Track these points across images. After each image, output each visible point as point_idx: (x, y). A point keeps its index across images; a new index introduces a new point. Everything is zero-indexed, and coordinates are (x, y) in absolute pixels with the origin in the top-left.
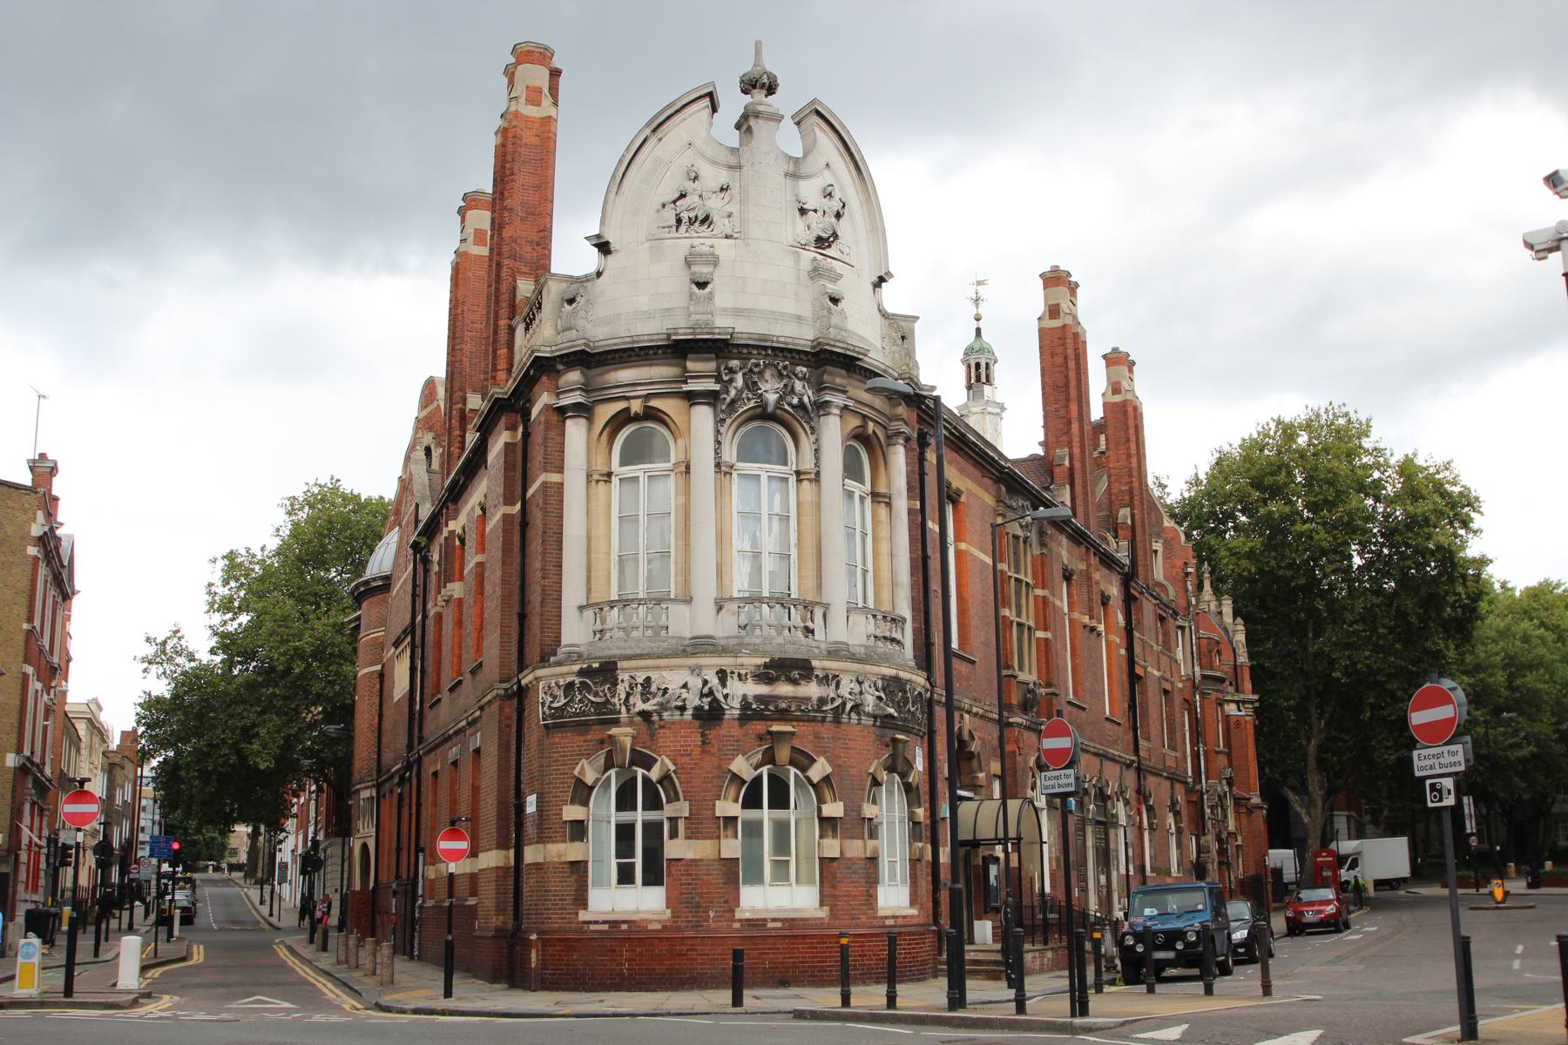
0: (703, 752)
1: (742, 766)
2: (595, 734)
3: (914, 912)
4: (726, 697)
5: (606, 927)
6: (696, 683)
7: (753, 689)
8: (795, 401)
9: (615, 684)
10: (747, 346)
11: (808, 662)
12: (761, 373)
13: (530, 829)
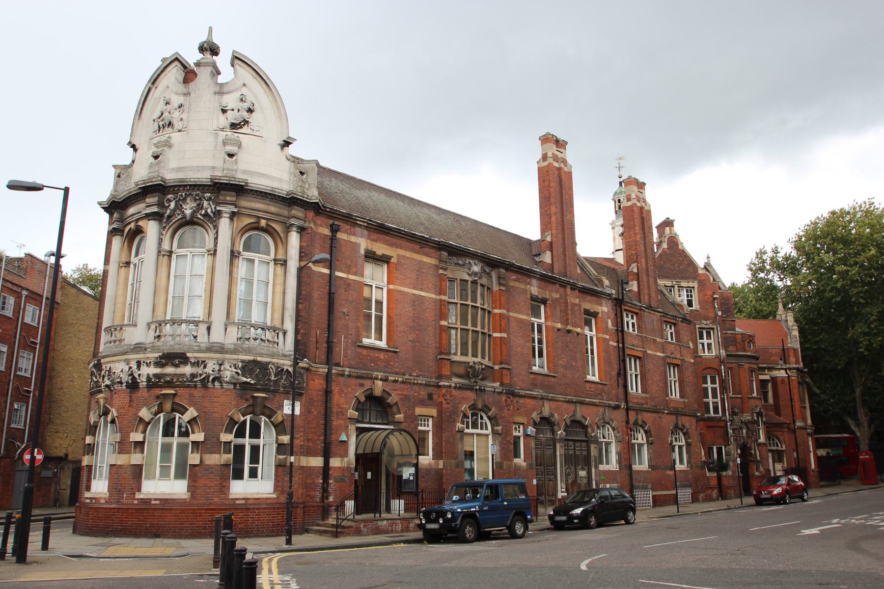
4: (139, 375)
6: (126, 368)
7: (153, 370)
8: (203, 212)
10: (175, 186)
11: (184, 354)
12: (184, 200)
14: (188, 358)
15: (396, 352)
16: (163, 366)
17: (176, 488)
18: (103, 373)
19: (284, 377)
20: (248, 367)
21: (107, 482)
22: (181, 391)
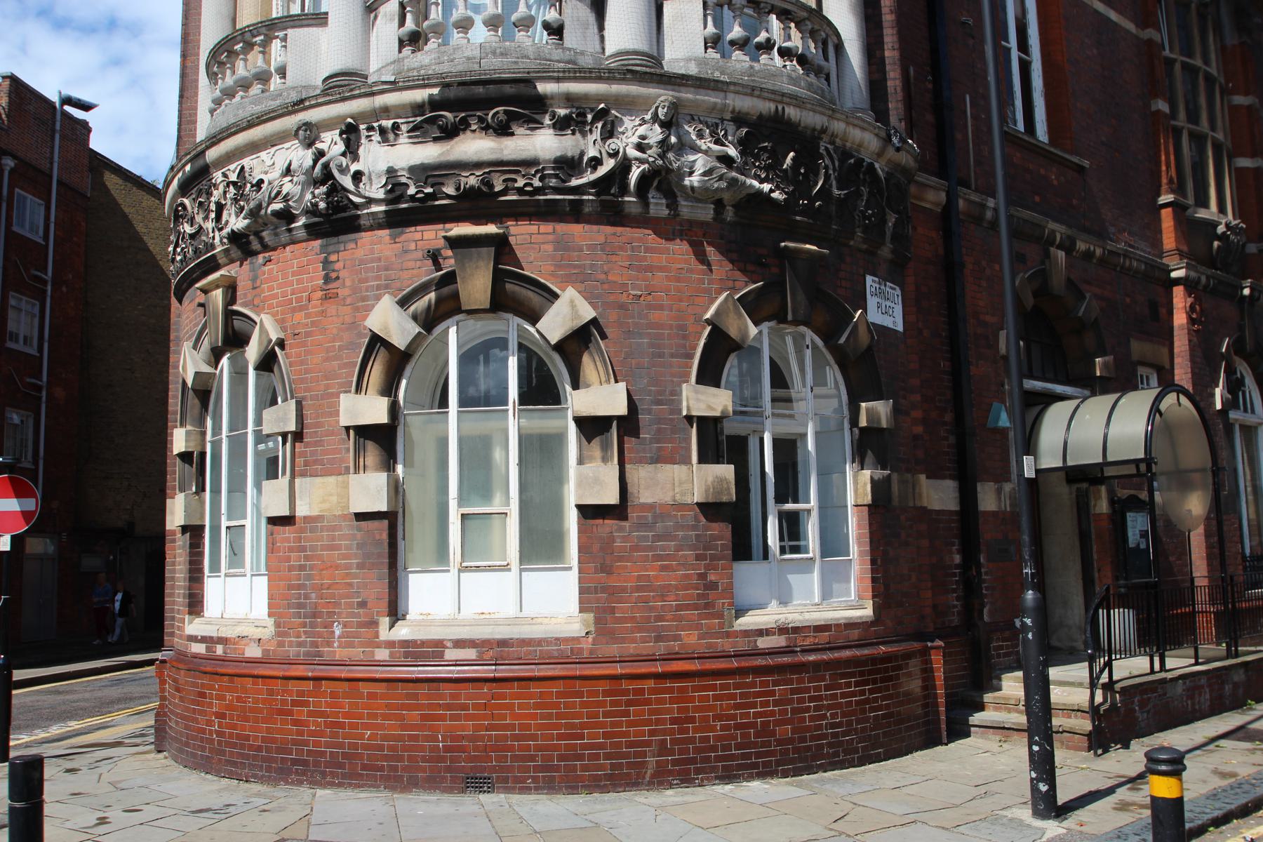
0: (326, 298)
1: (391, 322)
6: (307, 157)
7: (410, 153)
11: (529, 82)
15: (1080, 169)
16: (450, 133)
17: (547, 603)
18: (216, 195)
19: (864, 190)
20: (766, 135)
21: (262, 583)
22: (521, 233)
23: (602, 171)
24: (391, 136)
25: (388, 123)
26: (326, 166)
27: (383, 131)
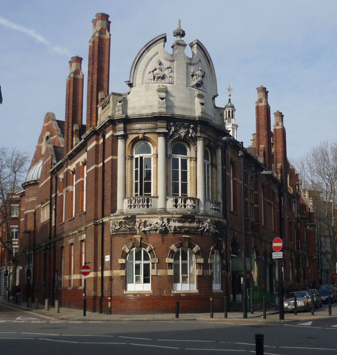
0: (162, 243)
1: (173, 247)
2: (129, 237)
3: (222, 291)
5: (132, 295)
7: (177, 224)
8: (190, 136)
9: (135, 222)
13: (107, 265)
14: (195, 219)
16: (183, 222)
23: (202, 229)
24: (175, 221)
25: (175, 219)
26: (165, 224)
27: (174, 220)
